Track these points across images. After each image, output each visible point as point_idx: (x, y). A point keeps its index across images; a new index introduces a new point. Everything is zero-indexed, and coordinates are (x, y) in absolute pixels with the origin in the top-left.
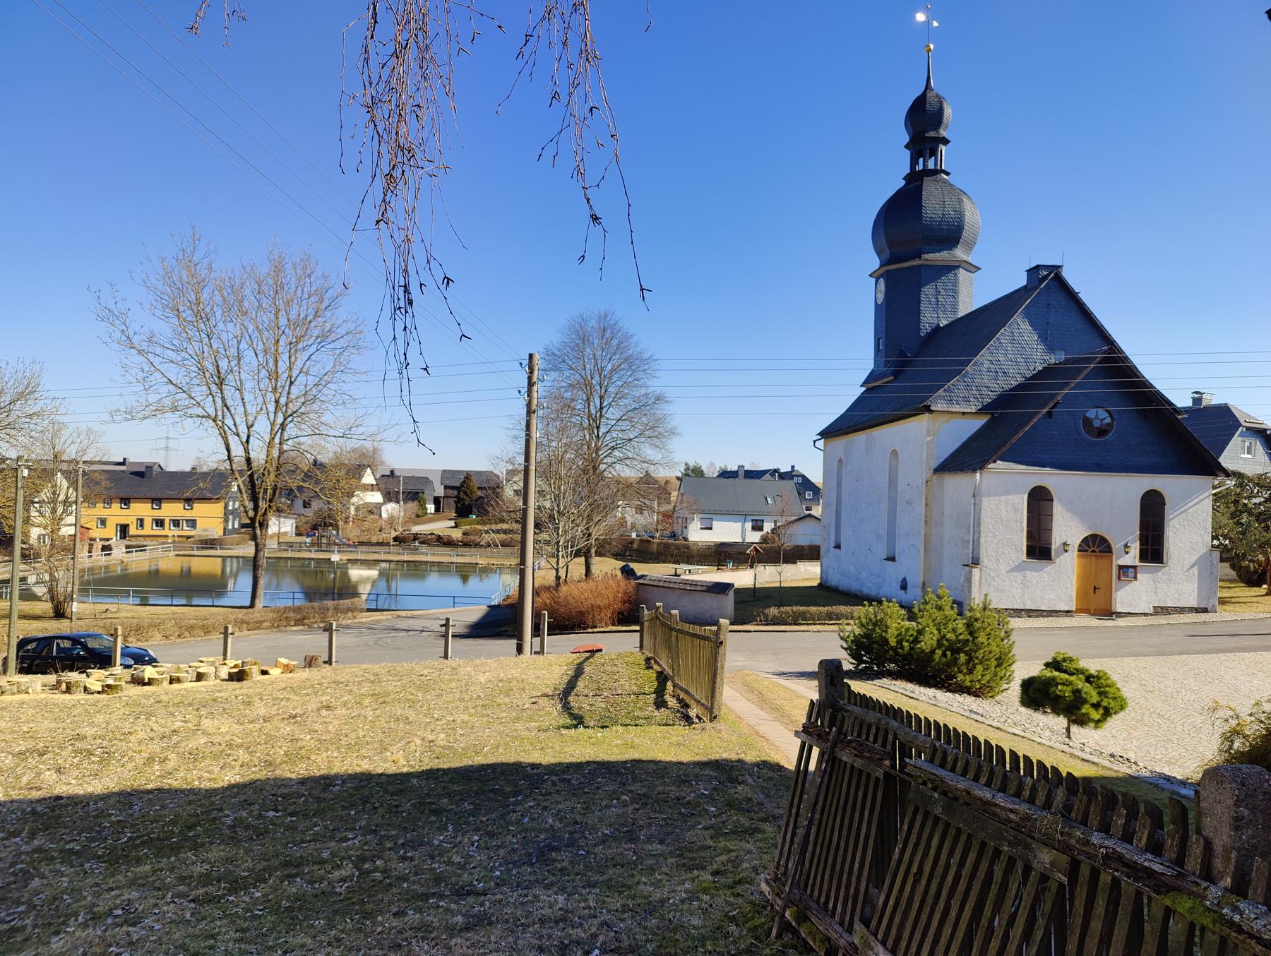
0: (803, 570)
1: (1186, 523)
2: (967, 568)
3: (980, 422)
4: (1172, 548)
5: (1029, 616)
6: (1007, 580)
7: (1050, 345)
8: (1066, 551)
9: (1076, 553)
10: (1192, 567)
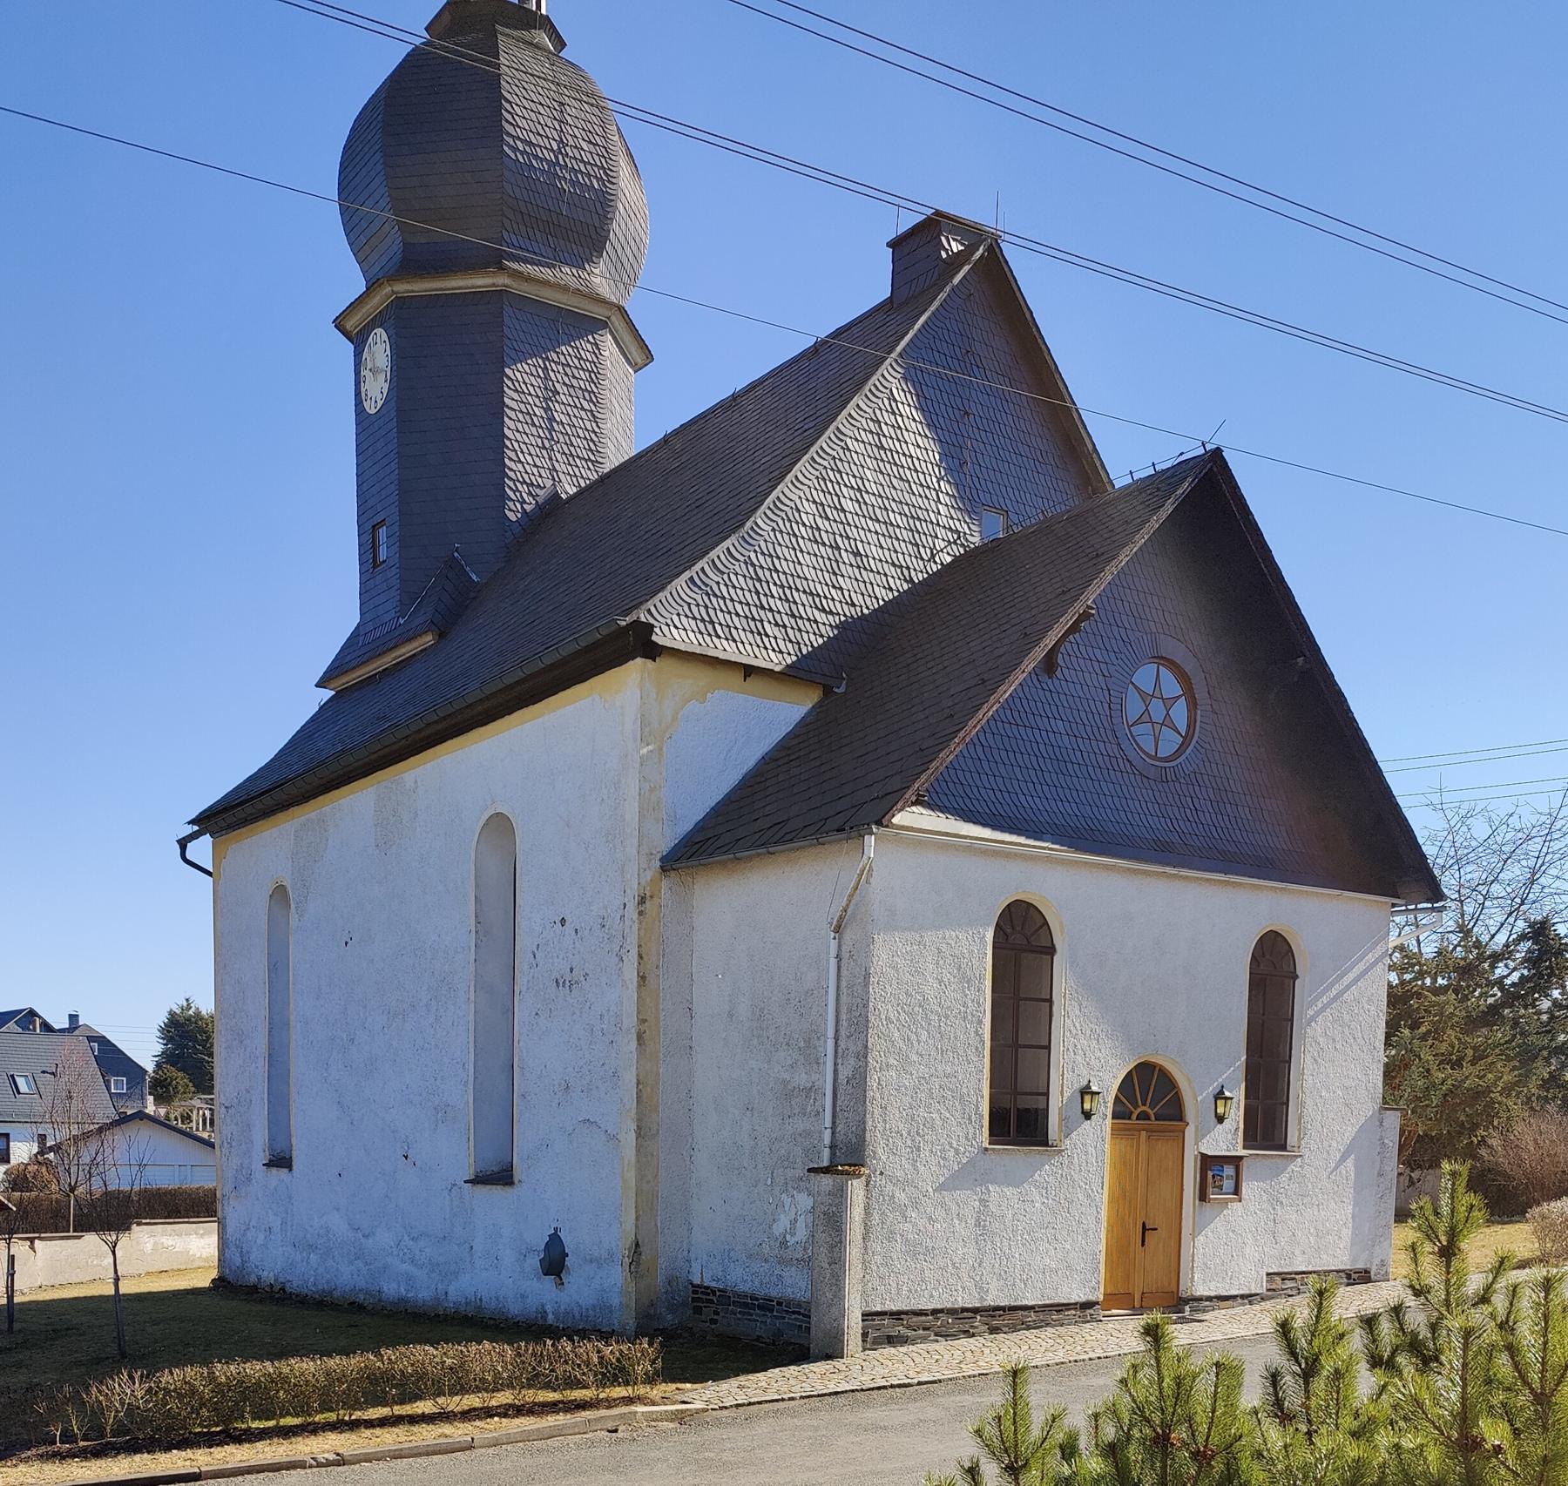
0: (149, 1246)
2: (826, 1181)
3: (791, 709)
4: (1309, 1110)
5: (994, 1330)
6: (940, 1213)
7: (970, 501)
8: (1087, 1115)
9: (1109, 1121)
10: (1344, 1158)
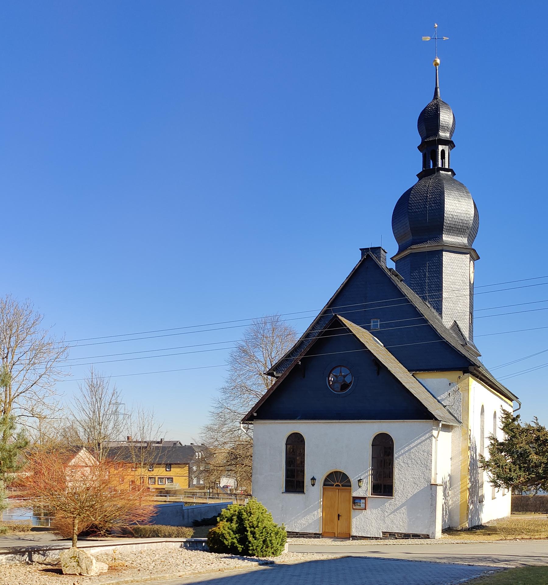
1: (409, 462)
